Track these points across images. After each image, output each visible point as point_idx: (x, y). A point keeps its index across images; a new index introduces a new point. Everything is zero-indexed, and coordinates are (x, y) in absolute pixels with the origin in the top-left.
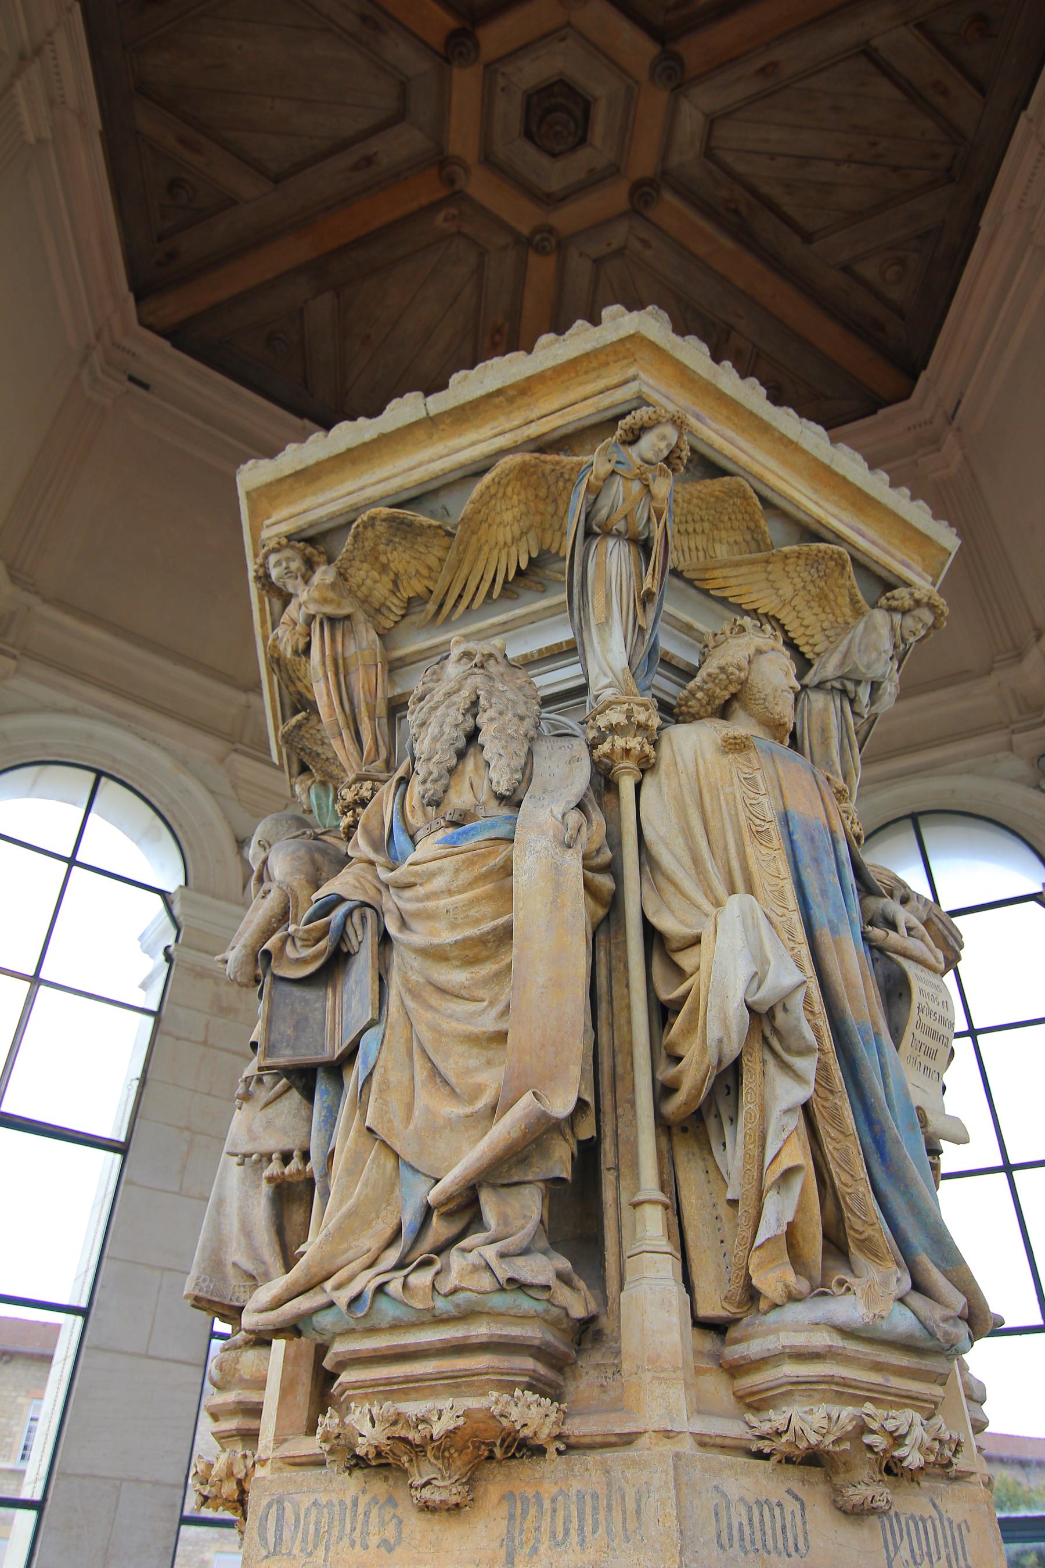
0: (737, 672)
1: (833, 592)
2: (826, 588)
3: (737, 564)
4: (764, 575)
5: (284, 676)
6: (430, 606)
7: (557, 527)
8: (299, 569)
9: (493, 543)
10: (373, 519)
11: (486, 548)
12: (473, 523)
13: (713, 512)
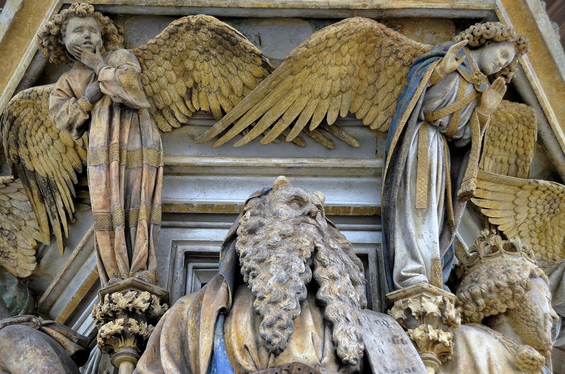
0: (523, 292)
1: (553, 228)
2: (549, 224)
3: (499, 182)
4: (512, 198)
5: (12, 136)
6: (208, 123)
7: (370, 96)
8: (98, 43)
9: (307, 90)
10: (201, 24)
11: (297, 92)
12: (295, 65)
13: (497, 129)
